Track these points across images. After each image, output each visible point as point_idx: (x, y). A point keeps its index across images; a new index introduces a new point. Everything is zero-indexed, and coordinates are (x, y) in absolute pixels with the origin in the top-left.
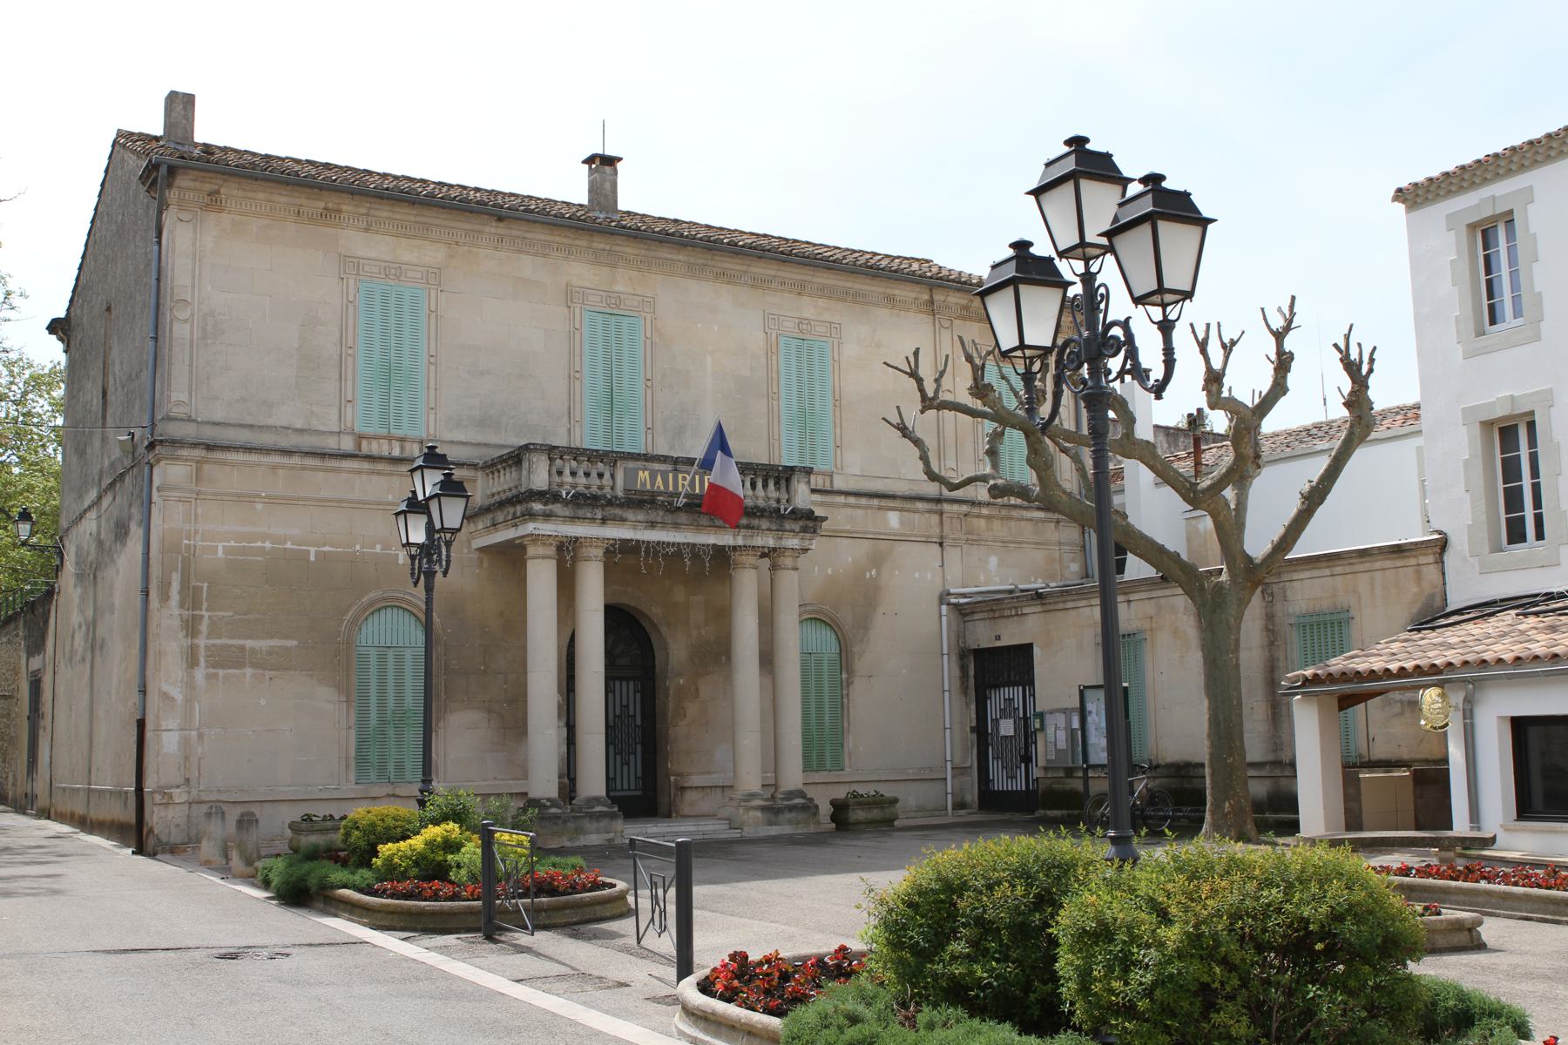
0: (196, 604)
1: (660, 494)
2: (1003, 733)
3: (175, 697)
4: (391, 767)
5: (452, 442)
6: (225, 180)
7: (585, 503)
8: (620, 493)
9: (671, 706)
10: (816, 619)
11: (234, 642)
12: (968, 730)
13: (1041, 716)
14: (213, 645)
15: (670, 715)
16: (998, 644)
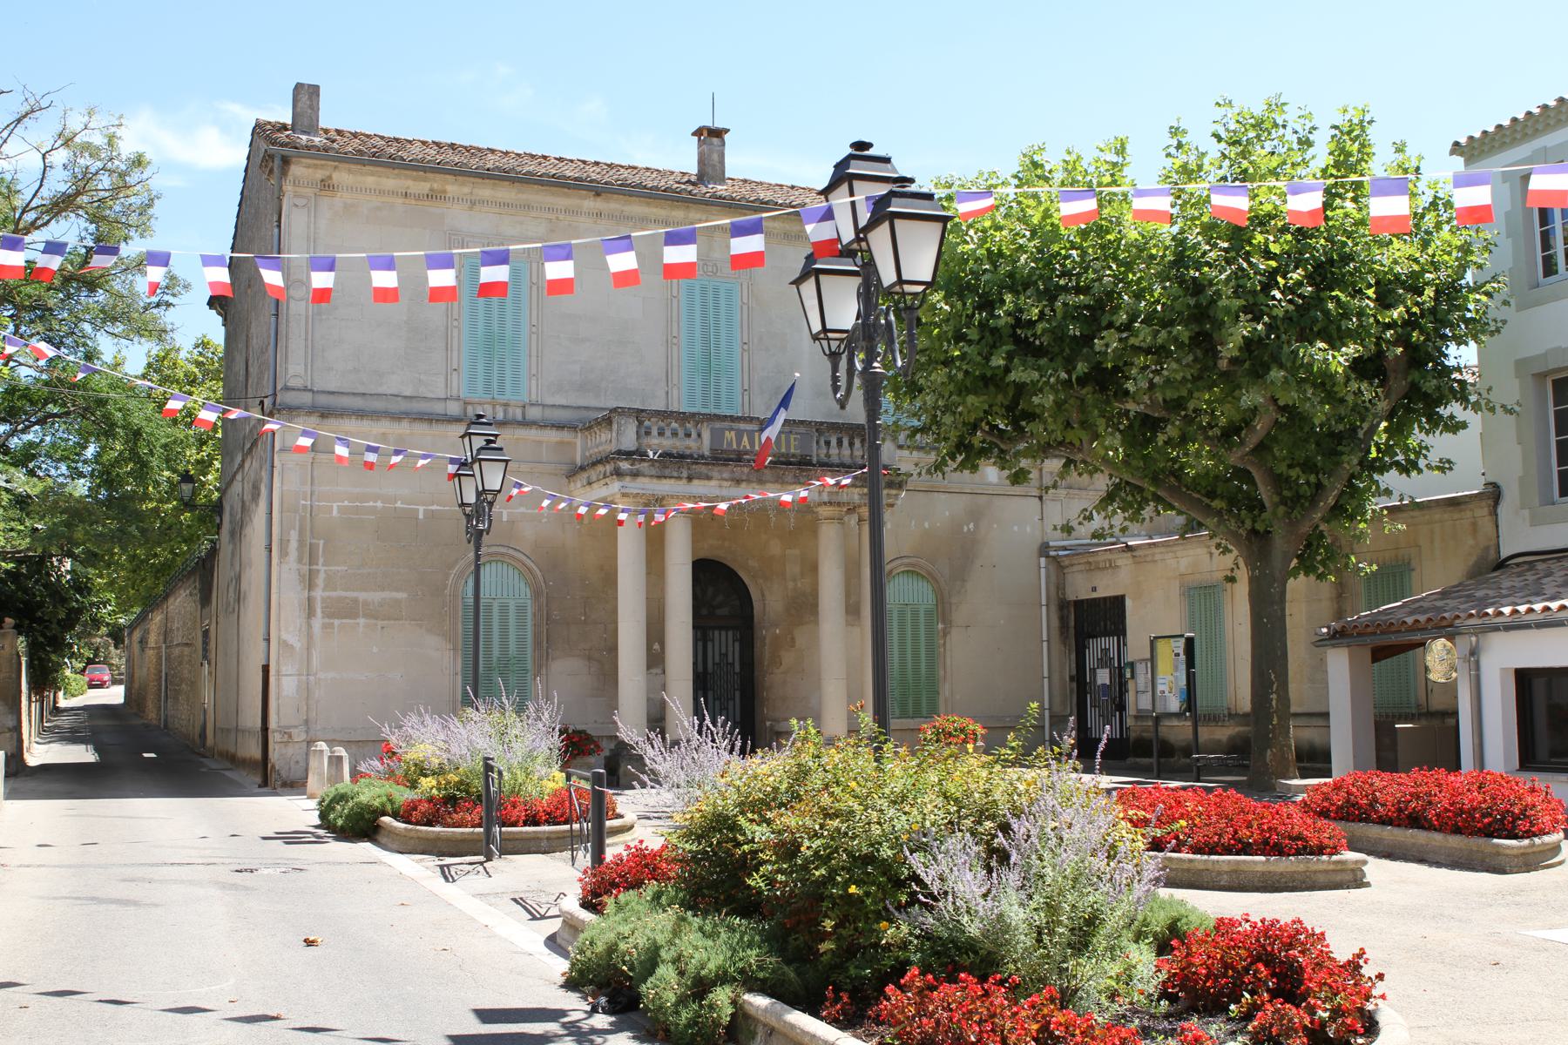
0: (312, 560)
1: (746, 454)
2: (1099, 682)
5: (553, 406)
6: (336, 167)
7: (674, 462)
8: (707, 453)
9: (767, 655)
10: (913, 572)
13: (1132, 665)
14: (329, 597)
16: (1095, 595)
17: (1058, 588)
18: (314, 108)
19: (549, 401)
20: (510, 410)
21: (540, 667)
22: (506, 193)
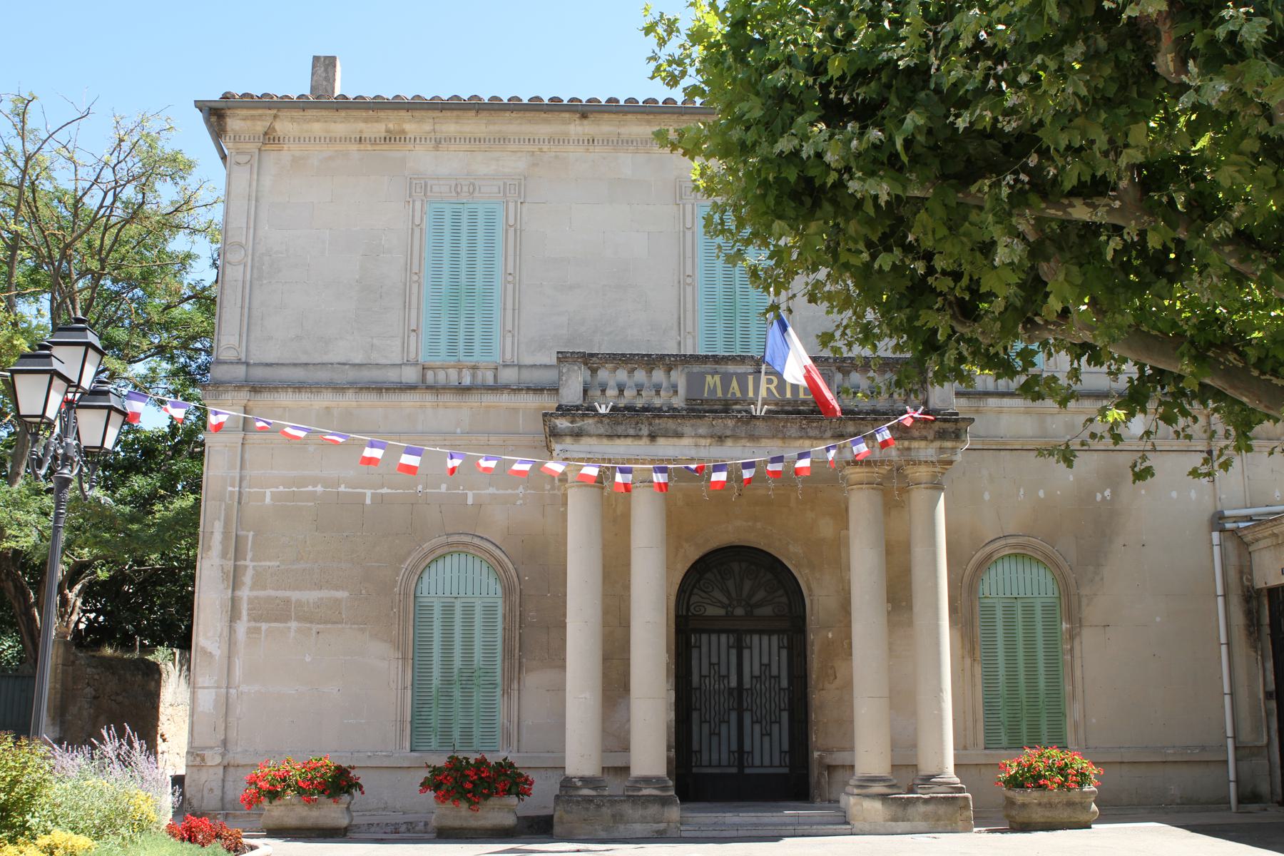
0: (239, 554)
3: (214, 653)
4: (456, 734)
5: (532, 366)
6: (275, 117)
10: (1023, 556)
11: (280, 593)
12: (1261, 696)
14: (257, 598)
15: (814, 676)
17: (1241, 573)
18: (330, 80)
19: (528, 360)
20: (479, 373)
21: (511, 680)
22: (473, 126)
